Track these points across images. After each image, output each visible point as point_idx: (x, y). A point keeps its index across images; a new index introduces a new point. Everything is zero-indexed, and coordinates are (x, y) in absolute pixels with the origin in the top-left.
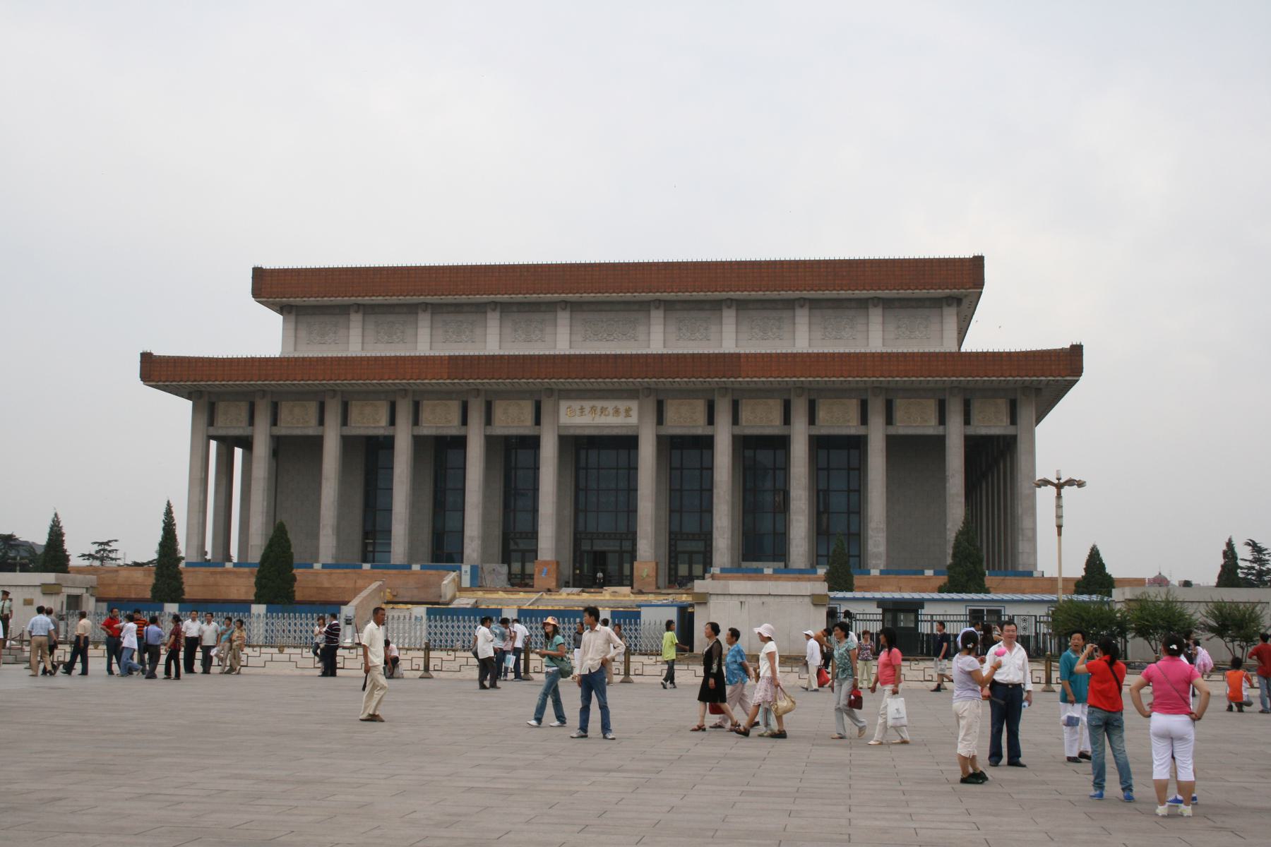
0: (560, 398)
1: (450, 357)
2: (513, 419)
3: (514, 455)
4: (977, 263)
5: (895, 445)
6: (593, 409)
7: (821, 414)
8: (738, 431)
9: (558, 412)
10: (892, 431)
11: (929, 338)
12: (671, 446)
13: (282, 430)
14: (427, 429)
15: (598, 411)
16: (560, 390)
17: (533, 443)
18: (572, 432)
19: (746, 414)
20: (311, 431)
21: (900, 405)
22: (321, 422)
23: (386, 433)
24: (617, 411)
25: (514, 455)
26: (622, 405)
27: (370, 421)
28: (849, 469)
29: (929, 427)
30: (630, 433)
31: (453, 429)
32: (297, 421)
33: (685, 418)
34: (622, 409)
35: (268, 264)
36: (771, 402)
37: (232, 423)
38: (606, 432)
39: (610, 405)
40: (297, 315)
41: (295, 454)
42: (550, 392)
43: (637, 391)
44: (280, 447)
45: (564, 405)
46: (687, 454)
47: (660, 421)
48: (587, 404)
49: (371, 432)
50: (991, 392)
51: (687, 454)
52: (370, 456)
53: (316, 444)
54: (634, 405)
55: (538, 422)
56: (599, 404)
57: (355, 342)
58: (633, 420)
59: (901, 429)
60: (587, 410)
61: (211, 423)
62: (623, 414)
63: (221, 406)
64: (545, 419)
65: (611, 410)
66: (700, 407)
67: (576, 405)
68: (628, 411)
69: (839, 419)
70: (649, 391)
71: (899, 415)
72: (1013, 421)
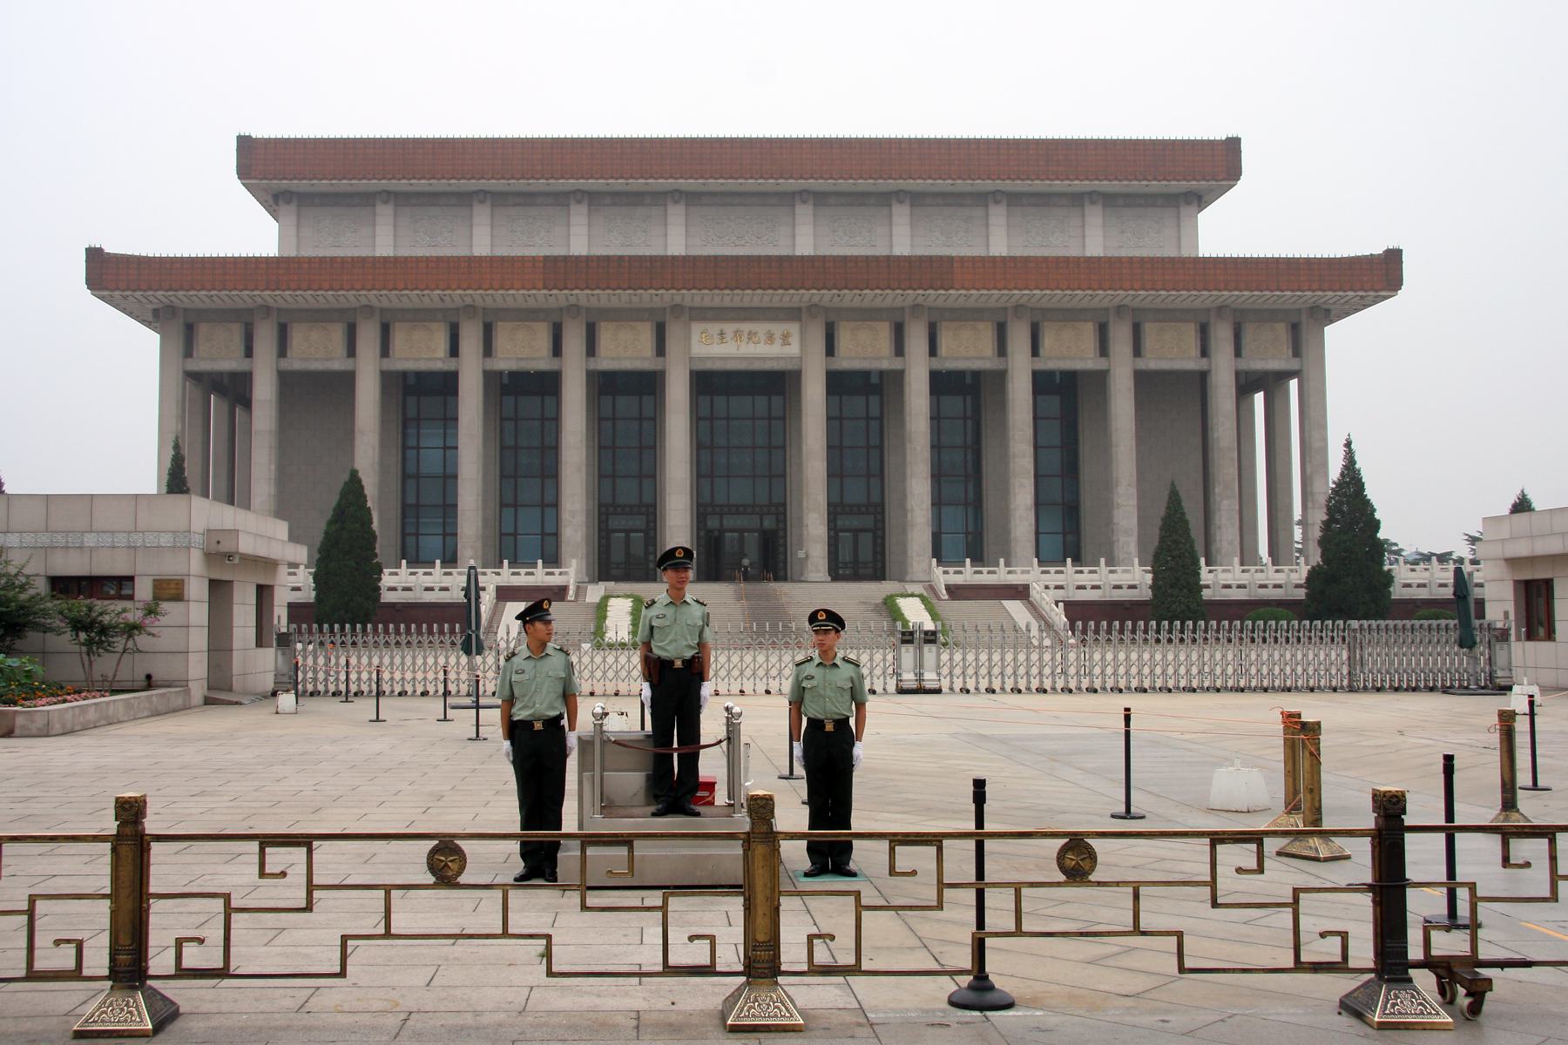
0: (691, 319)
1: (546, 258)
2: (625, 349)
3: (627, 397)
6: (737, 334)
7: (1048, 341)
8: (937, 364)
9: (688, 338)
10: (1142, 364)
11: (1142, 240)
12: (838, 383)
13: (294, 363)
14: (505, 361)
15: (745, 337)
16: (691, 309)
17: (648, 385)
18: (709, 366)
19: (946, 343)
20: (339, 364)
21: (1149, 329)
22: (352, 352)
23: (343, 368)
24: (770, 338)
25: (627, 397)
26: (778, 328)
27: (422, 351)
28: (965, 419)
30: (790, 367)
32: (316, 350)
33: (864, 349)
34: (777, 336)
35: (264, 129)
36: (981, 326)
37: (219, 354)
38: (757, 366)
39: (761, 328)
40: (1104, 206)
41: (316, 396)
42: (677, 310)
43: (799, 309)
44: (292, 385)
45: (697, 328)
46: (863, 397)
47: (830, 350)
48: (729, 328)
49: (422, 366)
50: (1269, 316)
51: (863, 397)
52: (421, 399)
53: (344, 383)
54: (793, 328)
55: (661, 350)
56: (746, 327)
57: (384, 238)
58: (794, 349)
59: (1151, 363)
60: (729, 335)
61: (188, 353)
62: (778, 341)
63: (203, 330)
64: (672, 346)
65: (762, 336)
66: (884, 332)
67: (714, 328)
68: (785, 339)
69: (1070, 350)
70: (813, 309)
71: (1149, 342)
72: (1297, 353)
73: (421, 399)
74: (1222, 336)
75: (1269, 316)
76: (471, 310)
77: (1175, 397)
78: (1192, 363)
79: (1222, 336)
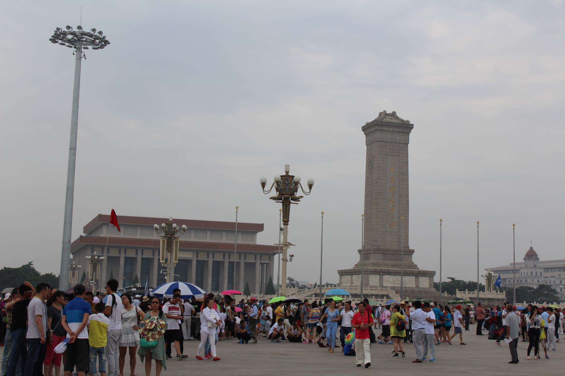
4: (263, 225)
5: (246, 264)
10: (246, 261)
20: (118, 255)
27: (131, 254)
29: (253, 261)
31: (151, 256)
39: (186, 253)
46: (202, 265)
47: (197, 257)
50: (267, 254)
53: (118, 258)
54: (191, 253)
58: (191, 256)
59: (247, 261)
70: (195, 250)
73: (130, 261)
74: (258, 257)
75: (267, 254)
76: (140, 248)
77: (250, 266)
78: (253, 261)
79: (258, 257)
